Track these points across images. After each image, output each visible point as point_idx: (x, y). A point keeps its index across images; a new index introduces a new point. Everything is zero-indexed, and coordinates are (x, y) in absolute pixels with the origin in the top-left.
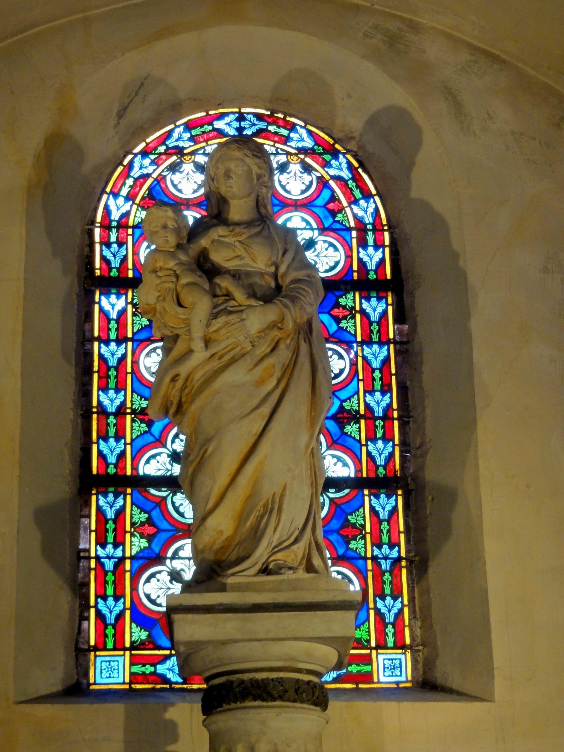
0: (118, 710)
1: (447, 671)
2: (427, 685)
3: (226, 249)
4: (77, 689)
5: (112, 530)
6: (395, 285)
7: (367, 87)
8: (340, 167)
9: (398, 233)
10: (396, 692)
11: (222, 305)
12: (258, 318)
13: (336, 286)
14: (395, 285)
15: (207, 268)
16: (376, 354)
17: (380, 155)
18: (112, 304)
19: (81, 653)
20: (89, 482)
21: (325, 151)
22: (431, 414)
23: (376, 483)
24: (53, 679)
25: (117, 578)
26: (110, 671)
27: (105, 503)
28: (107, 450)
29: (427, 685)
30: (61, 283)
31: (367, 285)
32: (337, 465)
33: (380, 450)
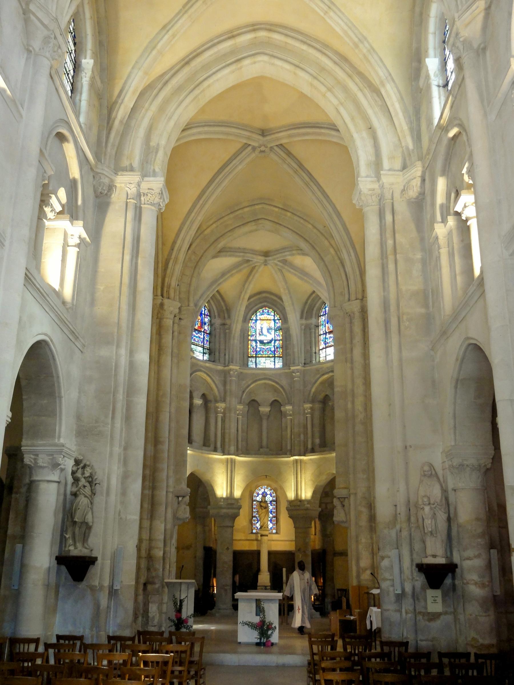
0: (255, 535)
1: (278, 532)
2: (277, 533)
3: (262, 504)
4: (252, 533)
5: (255, 521)
6: (276, 501)
7: (274, 485)
8: (272, 491)
9: (277, 497)
10: (274, 533)
11: (262, 509)
12: (264, 510)
13: (271, 501)
14: (276, 501)
15: (261, 506)
16: (274, 507)
17: (275, 490)
18: (254, 503)
19: (252, 530)
20: (253, 517)
21: (271, 490)
22: (278, 512)
23: (274, 517)
24: (250, 532)
25: (255, 524)
26: (254, 531)
27: (254, 518)
28: (254, 514)
29: (277, 533)
30: (251, 501)
31: (274, 501)
32: (271, 516)
33: (274, 514)
